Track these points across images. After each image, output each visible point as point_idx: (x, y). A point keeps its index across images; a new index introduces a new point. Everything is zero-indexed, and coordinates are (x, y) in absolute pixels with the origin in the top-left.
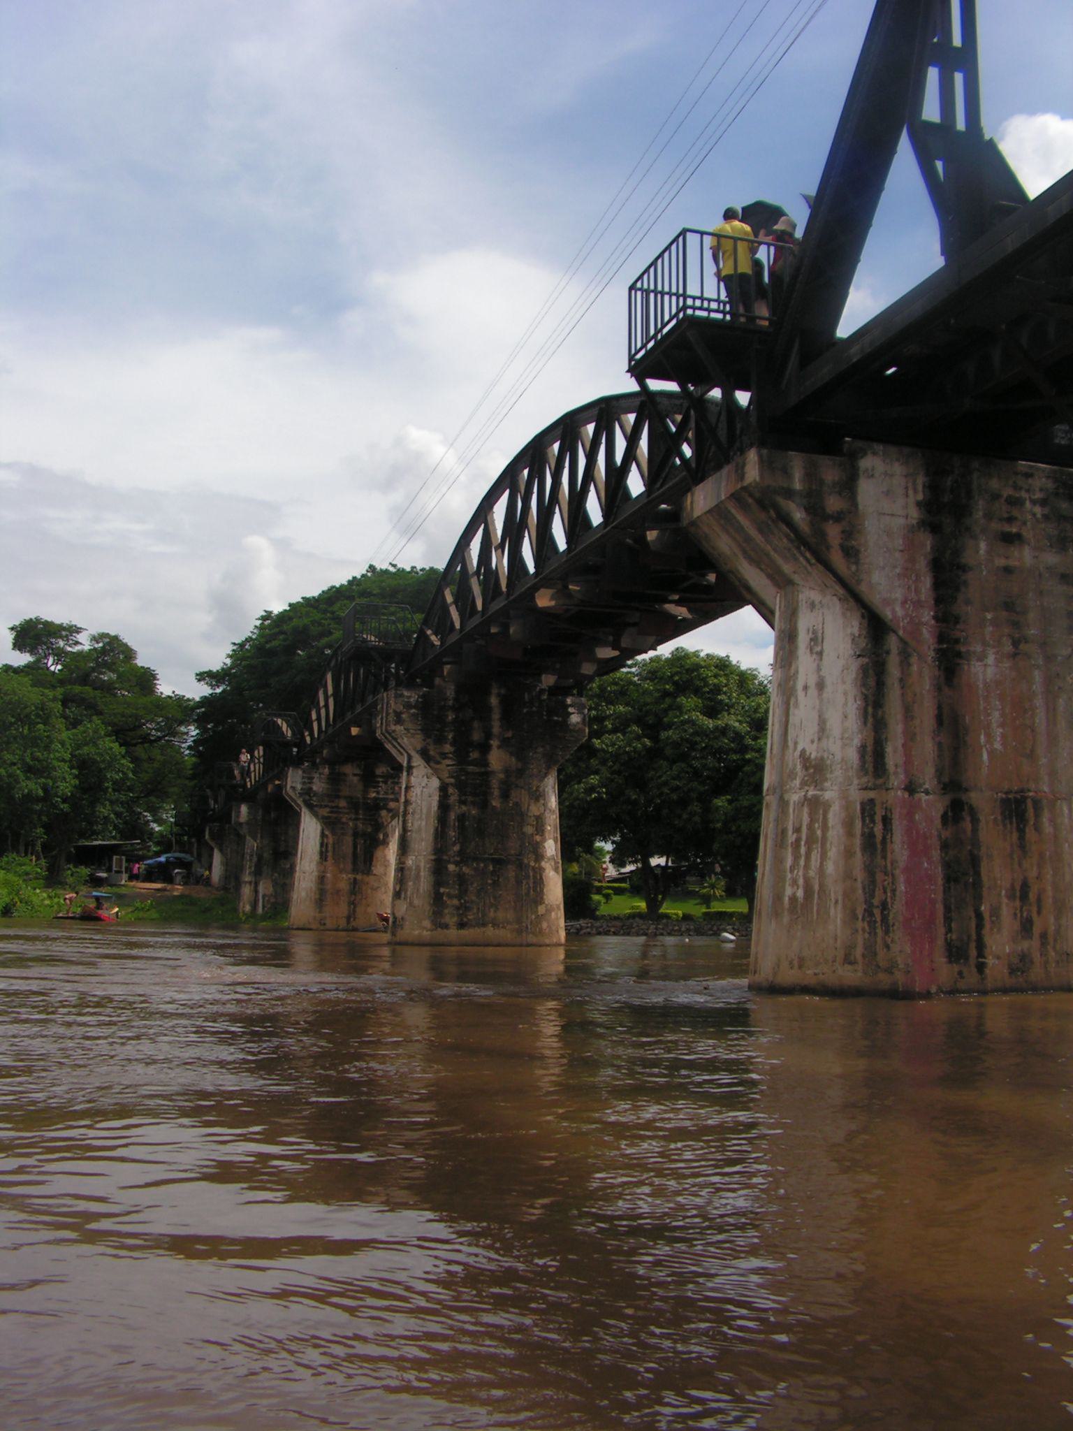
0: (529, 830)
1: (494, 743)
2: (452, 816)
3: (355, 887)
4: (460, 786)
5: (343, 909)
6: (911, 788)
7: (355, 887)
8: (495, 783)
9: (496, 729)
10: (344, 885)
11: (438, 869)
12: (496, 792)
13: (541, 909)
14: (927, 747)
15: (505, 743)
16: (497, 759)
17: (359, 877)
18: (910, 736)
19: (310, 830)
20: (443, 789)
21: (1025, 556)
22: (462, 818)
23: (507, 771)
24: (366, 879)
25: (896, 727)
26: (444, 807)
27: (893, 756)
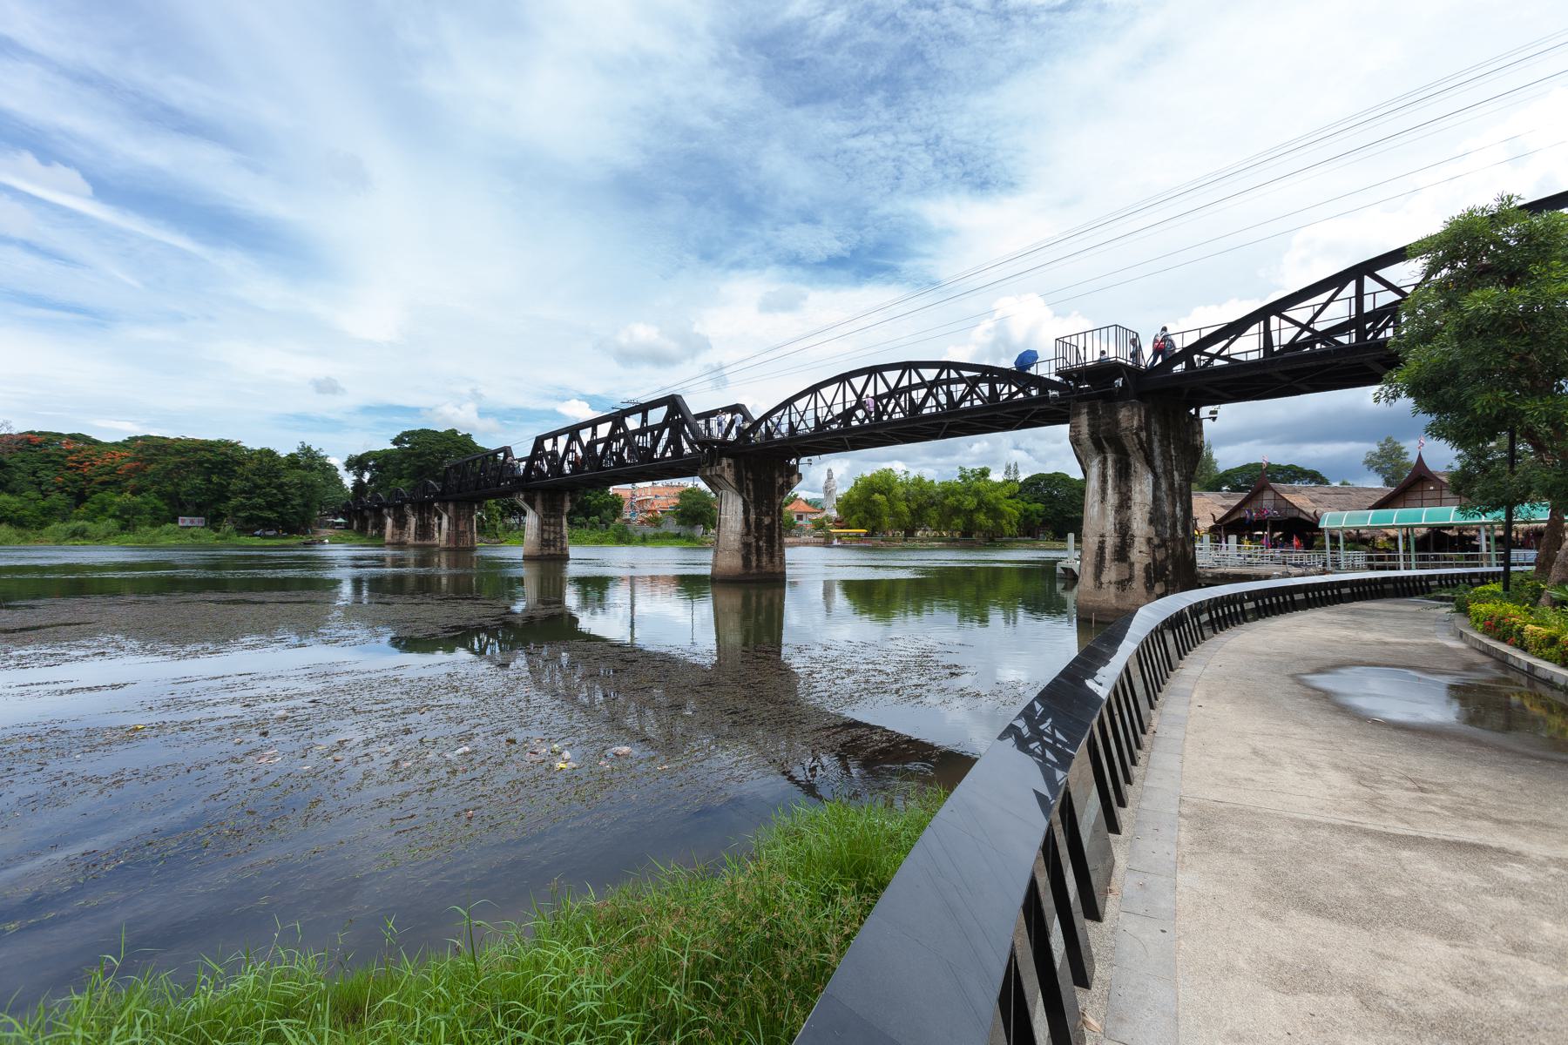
11: (416, 533)
16: (426, 515)
19: (389, 521)
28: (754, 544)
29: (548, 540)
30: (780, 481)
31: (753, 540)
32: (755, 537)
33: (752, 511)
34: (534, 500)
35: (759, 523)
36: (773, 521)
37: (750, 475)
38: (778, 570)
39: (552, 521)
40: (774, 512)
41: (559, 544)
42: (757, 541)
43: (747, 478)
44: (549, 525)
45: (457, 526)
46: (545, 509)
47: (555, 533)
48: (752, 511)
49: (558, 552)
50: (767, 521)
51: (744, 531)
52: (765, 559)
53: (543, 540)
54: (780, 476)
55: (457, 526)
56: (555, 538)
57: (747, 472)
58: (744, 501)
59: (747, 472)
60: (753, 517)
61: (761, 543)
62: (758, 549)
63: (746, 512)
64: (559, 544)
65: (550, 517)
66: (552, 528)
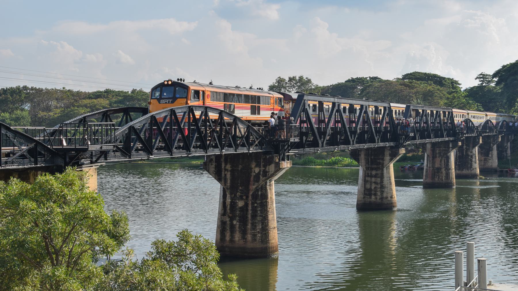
0: (470, 157)
1: (464, 145)
2: (457, 156)
3: (485, 160)
4: (459, 151)
5: (483, 163)
6: (430, 167)
7: (485, 160)
8: (465, 151)
9: (465, 143)
10: (483, 158)
12: (465, 152)
13: (472, 169)
14: (431, 164)
15: (466, 145)
17: (486, 157)
18: (430, 164)
20: (457, 152)
21: (441, 149)
22: (459, 156)
23: (466, 148)
24: (488, 158)
25: (429, 163)
26: (457, 154)
27: (428, 165)
28: (228, 222)
29: (370, 190)
30: (257, 170)
31: (228, 219)
32: (229, 217)
33: (228, 196)
34: (359, 155)
35: (233, 205)
36: (246, 205)
37: (228, 167)
38: (258, 245)
39: (374, 173)
40: (247, 197)
41: (379, 193)
42: (232, 219)
43: (226, 170)
44: (371, 176)
45: (433, 163)
46: (367, 162)
47: (376, 183)
48: (228, 196)
49: (379, 201)
50: (241, 204)
51: (223, 212)
52: (237, 236)
53: (365, 189)
54: (256, 166)
55: (433, 163)
56: (375, 188)
57: (226, 164)
58: (223, 188)
59: (226, 164)
60: (228, 200)
61: (235, 222)
62: (232, 227)
63: (224, 196)
64: (379, 193)
65: (372, 169)
66: (373, 180)
